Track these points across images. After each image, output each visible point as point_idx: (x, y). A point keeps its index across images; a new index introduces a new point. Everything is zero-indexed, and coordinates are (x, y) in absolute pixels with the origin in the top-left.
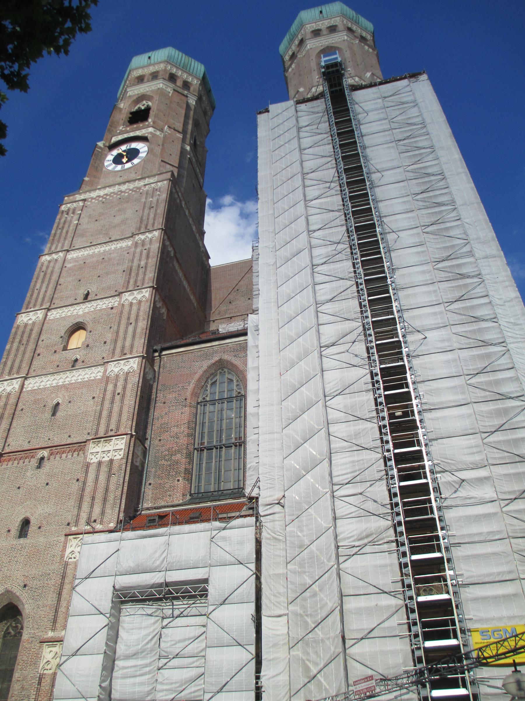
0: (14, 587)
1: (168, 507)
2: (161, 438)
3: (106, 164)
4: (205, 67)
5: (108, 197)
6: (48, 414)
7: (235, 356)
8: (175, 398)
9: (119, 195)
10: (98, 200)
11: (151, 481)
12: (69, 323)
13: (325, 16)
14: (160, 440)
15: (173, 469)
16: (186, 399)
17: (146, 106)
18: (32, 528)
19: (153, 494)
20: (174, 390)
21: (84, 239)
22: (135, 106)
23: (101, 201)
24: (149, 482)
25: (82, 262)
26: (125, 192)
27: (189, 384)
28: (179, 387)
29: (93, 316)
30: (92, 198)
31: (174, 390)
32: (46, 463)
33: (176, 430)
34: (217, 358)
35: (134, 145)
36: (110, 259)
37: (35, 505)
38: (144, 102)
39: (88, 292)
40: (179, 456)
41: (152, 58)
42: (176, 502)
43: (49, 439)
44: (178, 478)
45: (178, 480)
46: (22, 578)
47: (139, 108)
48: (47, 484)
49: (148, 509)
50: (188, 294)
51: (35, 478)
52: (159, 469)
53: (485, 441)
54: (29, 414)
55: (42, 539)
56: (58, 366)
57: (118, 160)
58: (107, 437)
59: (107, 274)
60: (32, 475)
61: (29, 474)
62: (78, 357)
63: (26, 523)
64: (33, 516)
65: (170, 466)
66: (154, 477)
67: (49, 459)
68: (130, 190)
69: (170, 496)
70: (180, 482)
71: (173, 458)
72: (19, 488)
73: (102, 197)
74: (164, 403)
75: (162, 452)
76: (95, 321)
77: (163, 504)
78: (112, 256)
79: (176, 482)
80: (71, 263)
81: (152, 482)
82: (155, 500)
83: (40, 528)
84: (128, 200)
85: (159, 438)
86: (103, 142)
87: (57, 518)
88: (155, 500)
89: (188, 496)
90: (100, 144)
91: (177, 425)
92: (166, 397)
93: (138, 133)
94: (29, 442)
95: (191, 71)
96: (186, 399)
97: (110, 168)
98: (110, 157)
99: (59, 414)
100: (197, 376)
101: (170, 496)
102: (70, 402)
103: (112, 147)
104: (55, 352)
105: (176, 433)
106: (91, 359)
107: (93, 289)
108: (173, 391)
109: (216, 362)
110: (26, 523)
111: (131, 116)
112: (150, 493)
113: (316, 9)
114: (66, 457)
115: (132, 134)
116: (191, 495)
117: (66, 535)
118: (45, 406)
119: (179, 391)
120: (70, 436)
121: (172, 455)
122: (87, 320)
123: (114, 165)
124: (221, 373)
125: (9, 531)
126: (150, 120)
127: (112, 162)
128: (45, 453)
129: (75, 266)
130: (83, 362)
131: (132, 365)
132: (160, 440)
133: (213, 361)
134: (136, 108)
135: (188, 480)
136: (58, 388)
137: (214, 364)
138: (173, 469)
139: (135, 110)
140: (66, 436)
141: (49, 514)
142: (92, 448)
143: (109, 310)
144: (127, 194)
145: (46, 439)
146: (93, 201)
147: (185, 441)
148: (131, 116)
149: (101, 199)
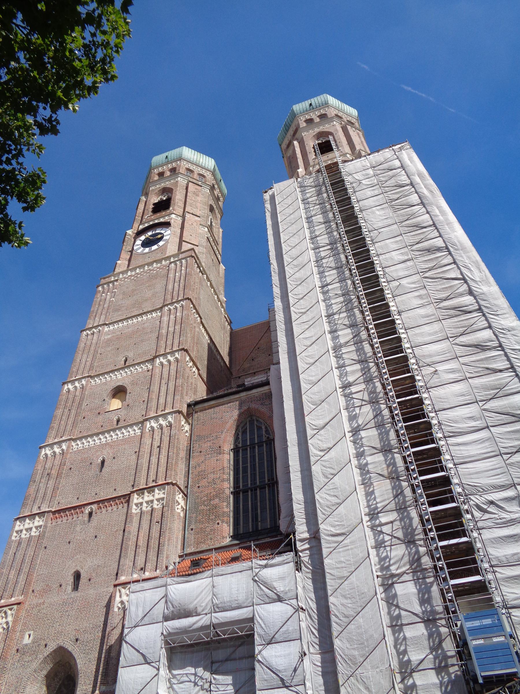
0: (66, 643)
2: (200, 485)
4: (215, 161)
5: (139, 276)
7: (262, 404)
11: (193, 526)
13: (314, 107)
15: (213, 513)
16: (220, 447)
18: (83, 581)
19: (195, 538)
20: (209, 439)
21: (120, 313)
24: (191, 527)
26: (153, 270)
27: (222, 433)
29: (132, 379)
30: (125, 278)
31: (209, 439)
33: (212, 476)
36: (144, 328)
37: (84, 559)
41: (169, 157)
43: (96, 494)
45: (218, 524)
46: (74, 633)
47: (161, 199)
48: (96, 537)
50: (215, 355)
52: (200, 514)
53: (507, 462)
54: (77, 473)
55: (91, 591)
56: (102, 426)
57: (146, 244)
58: (150, 489)
59: (142, 341)
60: (81, 529)
61: (78, 529)
63: (77, 576)
64: (82, 569)
66: (196, 522)
69: (211, 539)
72: (69, 543)
73: (134, 276)
74: (201, 452)
75: (201, 498)
76: (133, 383)
78: (146, 325)
79: (217, 526)
80: (109, 335)
81: (194, 527)
82: (198, 544)
83: (90, 580)
84: (155, 277)
85: (198, 485)
86: (131, 230)
87: (105, 569)
88: (198, 544)
89: (228, 537)
90: (129, 232)
94: (78, 499)
97: (139, 251)
98: (139, 242)
101: (211, 539)
102: (114, 458)
103: (139, 233)
104: (99, 413)
106: (132, 417)
107: (130, 355)
110: (77, 576)
112: (193, 538)
113: (306, 102)
117: (115, 586)
118: (91, 464)
119: (213, 440)
120: (115, 490)
122: (126, 383)
123: (142, 248)
125: (61, 586)
126: (171, 208)
128: (94, 507)
129: (113, 336)
130: (124, 420)
132: (199, 487)
134: (159, 199)
136: (103, 446)
138: (213, 513)
140: (112, 490)
141: (98, 566)
142: (135, 499)
145: (93, 494)
146: (126, 280)
149: (133, 278)
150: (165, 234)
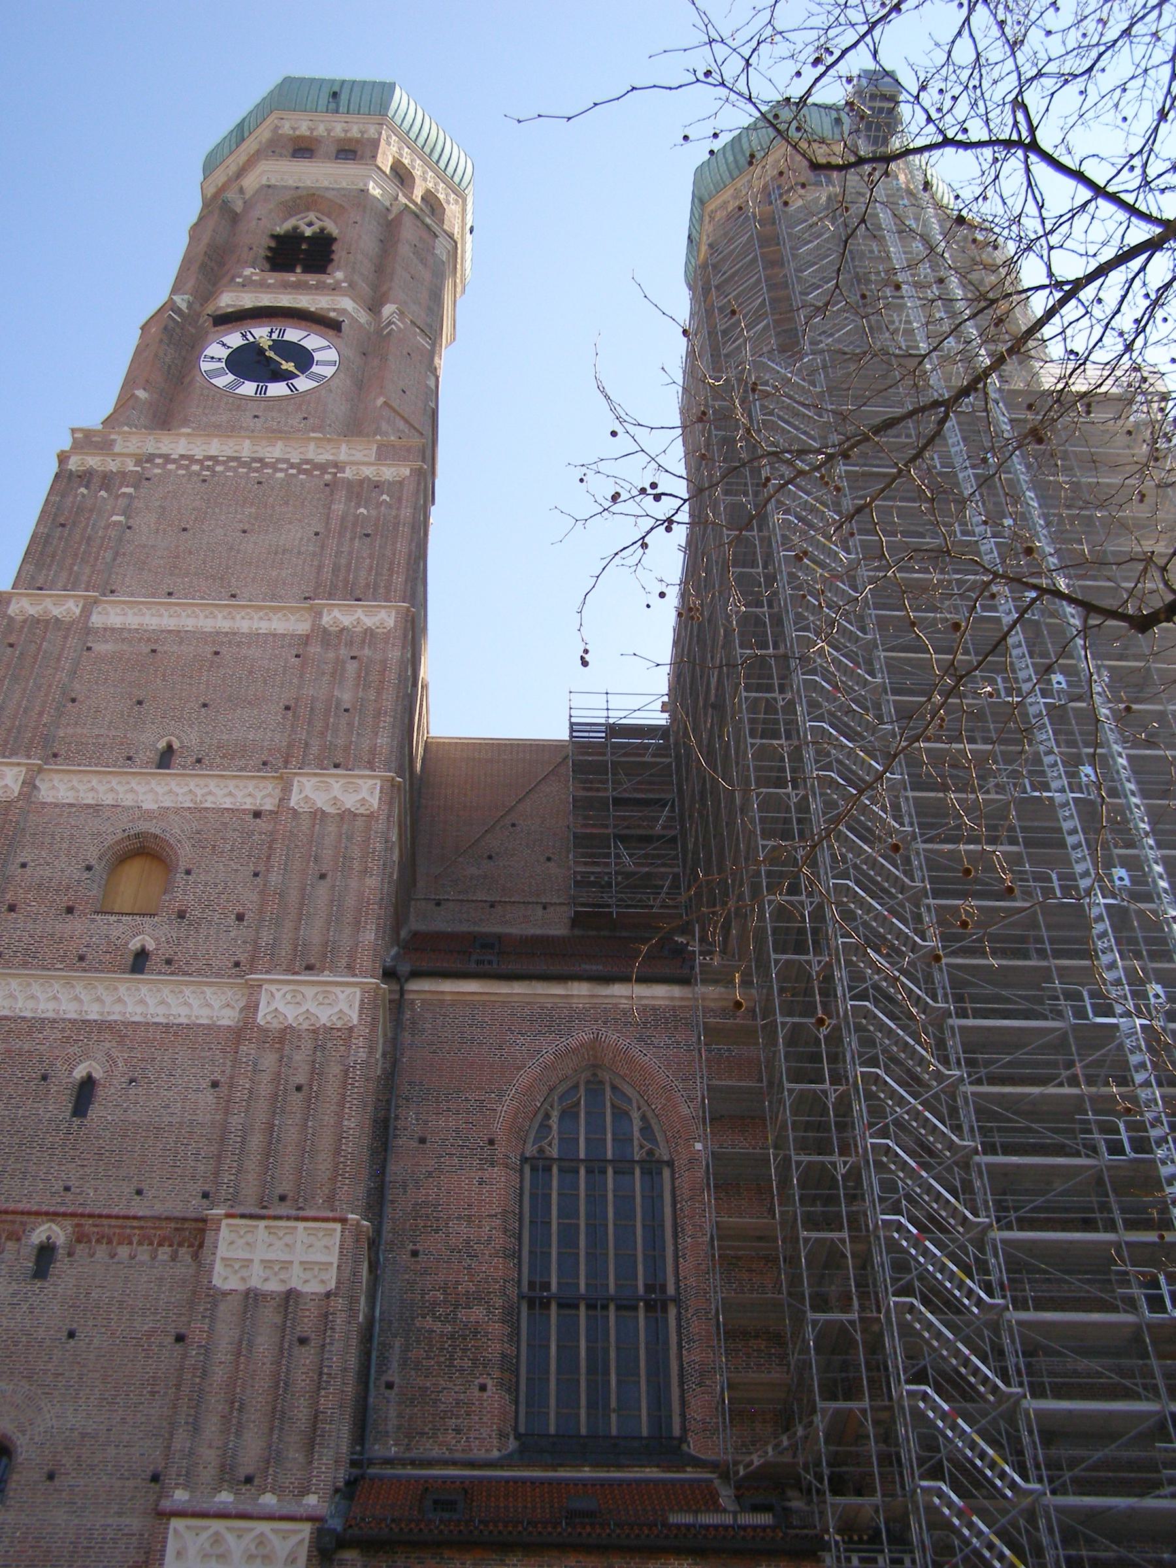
1: (454, 1463)
2: (418, 1247)
3: (205, 366)
6: (59, 1105)
8: (457, 1131)
9: (256, 470)
10: (187, 467)
11: (393, 1375)
12: (114, 832)
14: (415, 1254)
15: (464, 1350)
16: (491, 1142)
17: (315, 228)
22: (285, 220)
23: (198, 474)
25: (145, 649)
27: (500, 1096)
28: (467, 1100)
30: (167, 458)
32: (61, 1265)
33: (463, 1228)
34: (585, 1036)
35: (313, 342)
38: (312, 216)
39: (170, 747)
40: (478, 1313)
42: (479, 1454)
43: (67, 1189)
44: (481, 1381)
47: (295, 228)
49: (389, 1462)
51: (25, 1307)
52: (418, 1341)
60: (14, 1295)
62: (151, 945)
64: (24, 1432)
65: (452, 1337)
67: (70, 1255)
68: (292, 466)
70: (489, 1393)
71: (462, 1314)
77: (436, 1453)
79: (477, 1393)
81: (396, 1379)
83: (51, 1477)
85: (411, 1247)
89: (512, 1438)
91: (470, 1216)
92: (426, 1122)
93: (303, 301)
95: (442, 164)
96: (491, 1142)
99: (95, 1112)
100: (523, 1078)
101: (458, 1431)
105: (467, 1241)
108: (449, 1110)
109: (582, 1045)
111: (273, 244)
112: (392, 1413)
114: (132, 1257)
115: (285, 300)
116: (518, 1436)
121: (456, 1306)
122: (175, 831)
123: (230, 377)
124: (588, 1082)
127: (223, 365)
131: (343, 1006)
133: (573, 1042)
135: (509, 1390)
137: (575, 1051)
139: (282, 232)
140: (128, 1189)
141: (83, 1435)
143: (249, 818)
144: (280, 475)
145: (58, 1186)
147: (496, 1268)
148: (273, 244)
150: (317, 356)
